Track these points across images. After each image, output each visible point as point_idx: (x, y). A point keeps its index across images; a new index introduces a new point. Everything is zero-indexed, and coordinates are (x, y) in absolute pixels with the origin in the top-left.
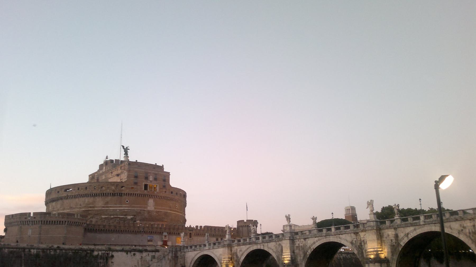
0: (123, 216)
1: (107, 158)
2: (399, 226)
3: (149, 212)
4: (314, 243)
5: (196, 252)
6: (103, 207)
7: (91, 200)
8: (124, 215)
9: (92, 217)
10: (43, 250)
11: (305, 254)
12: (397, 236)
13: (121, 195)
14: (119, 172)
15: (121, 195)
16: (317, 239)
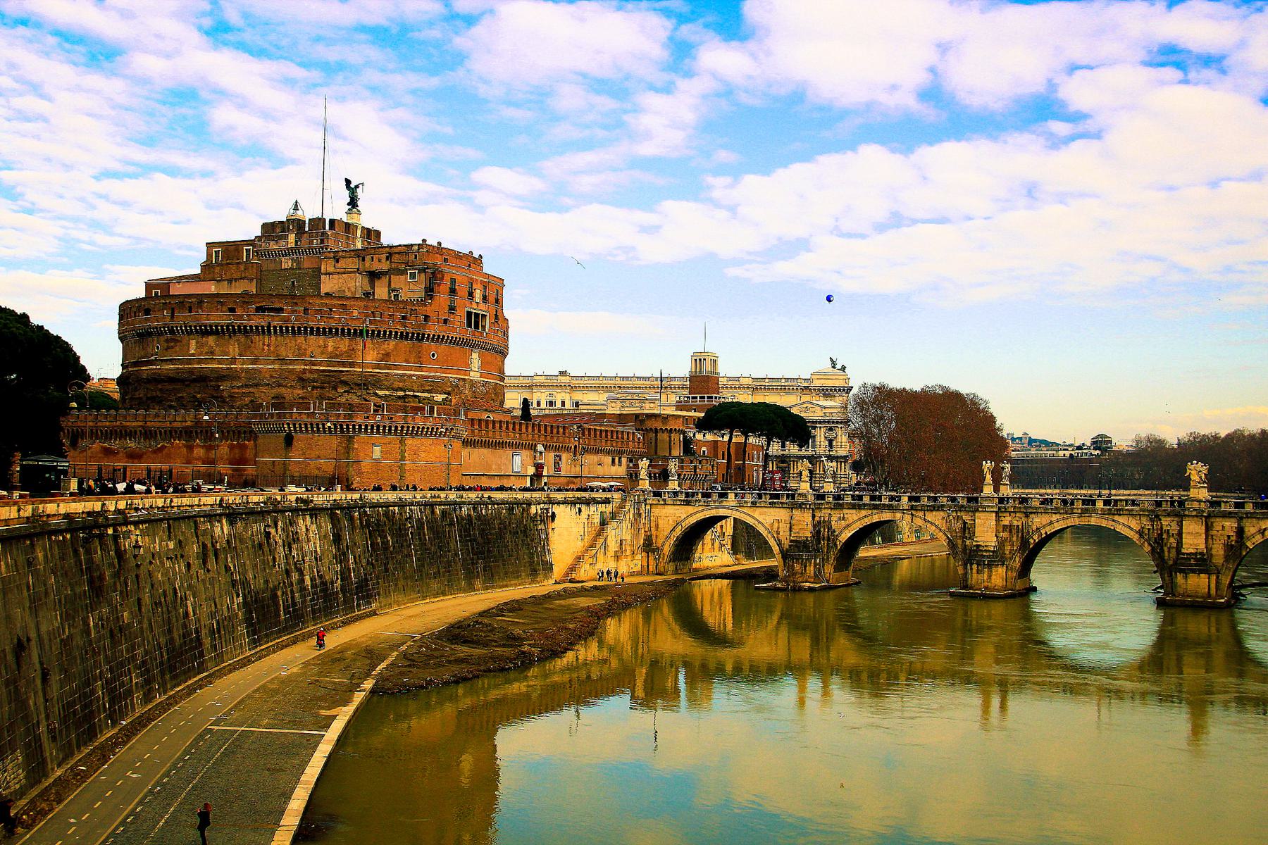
0: (426, 395)
1: (296, 207)
2: (1249, 516)
3: (472, 384)
4: (1051, 523)
5: (690, 509)
6: (378, 366)
7: (344, 344)
8: (429, 391)
9: (348, 392)
10: (475, 505)
11: (1024, 542)
12: (1240, 532)
13: (420, 338)
14: (385, 266)
15: (420, 338)
16: (1055, 517)
